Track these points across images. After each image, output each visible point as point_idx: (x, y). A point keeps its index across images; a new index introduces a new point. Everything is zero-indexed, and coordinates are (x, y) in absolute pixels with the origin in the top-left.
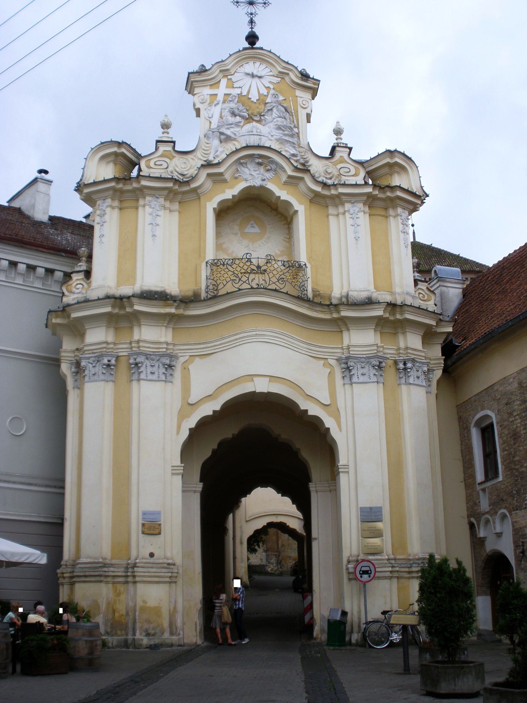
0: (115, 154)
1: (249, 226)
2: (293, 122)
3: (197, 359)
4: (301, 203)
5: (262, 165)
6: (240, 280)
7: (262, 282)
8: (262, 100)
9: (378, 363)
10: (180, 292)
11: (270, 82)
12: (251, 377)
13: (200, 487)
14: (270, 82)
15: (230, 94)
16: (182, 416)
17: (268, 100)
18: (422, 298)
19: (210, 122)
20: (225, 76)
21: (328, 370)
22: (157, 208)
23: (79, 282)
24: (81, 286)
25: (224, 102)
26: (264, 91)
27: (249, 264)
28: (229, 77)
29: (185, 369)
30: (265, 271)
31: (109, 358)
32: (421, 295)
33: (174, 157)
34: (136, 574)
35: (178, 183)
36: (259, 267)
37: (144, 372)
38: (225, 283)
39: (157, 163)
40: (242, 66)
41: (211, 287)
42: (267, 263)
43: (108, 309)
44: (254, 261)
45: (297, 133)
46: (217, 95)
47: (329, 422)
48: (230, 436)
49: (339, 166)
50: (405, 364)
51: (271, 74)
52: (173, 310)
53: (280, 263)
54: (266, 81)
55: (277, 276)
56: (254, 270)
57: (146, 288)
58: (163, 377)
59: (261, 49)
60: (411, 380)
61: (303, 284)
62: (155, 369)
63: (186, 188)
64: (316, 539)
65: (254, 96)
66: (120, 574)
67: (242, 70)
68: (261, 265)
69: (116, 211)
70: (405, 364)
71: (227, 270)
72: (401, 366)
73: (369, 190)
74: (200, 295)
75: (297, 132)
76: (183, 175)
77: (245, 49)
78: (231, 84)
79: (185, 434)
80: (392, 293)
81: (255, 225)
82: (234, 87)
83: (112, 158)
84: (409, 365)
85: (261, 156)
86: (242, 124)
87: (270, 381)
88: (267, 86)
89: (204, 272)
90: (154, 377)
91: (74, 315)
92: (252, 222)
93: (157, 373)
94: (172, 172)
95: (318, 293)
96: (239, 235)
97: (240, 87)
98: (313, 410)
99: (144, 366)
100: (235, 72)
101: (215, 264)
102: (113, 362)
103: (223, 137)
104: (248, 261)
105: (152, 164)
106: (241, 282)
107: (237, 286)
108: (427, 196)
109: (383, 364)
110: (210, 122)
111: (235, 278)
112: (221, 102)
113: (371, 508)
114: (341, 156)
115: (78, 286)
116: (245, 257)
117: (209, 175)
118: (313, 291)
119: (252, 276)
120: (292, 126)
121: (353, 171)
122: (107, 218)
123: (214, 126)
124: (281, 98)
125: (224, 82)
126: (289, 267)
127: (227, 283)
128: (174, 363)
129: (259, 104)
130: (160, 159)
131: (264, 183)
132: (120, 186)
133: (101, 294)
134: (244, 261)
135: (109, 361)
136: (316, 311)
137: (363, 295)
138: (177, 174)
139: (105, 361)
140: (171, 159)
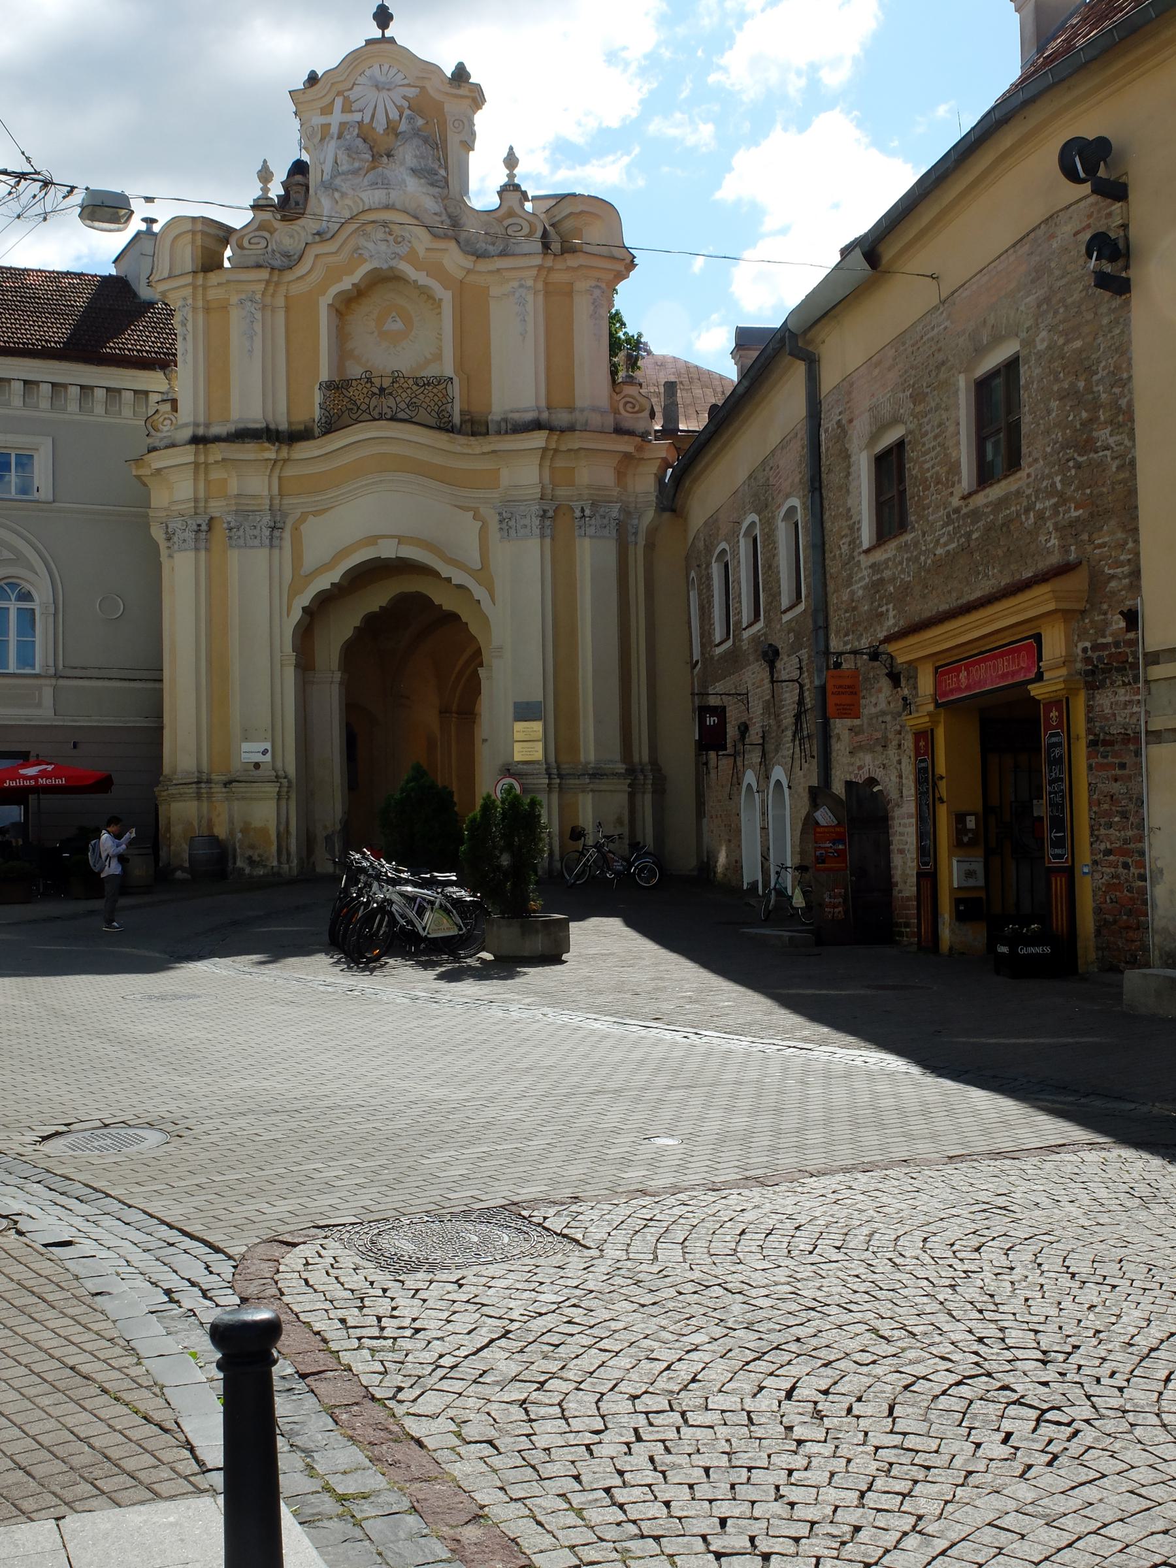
0: (194, 233)
1: (390, 320)
2: (439, 160)
3: (311, 517)
4: (446, 288)
5: (391, 235)
6: (358, 408)
7: (386, 410)
8: (392, 128)
9: (542, 513)
10: (290, 423)
11: (404, 97)
12: (372, 540)
13: (338, 676)
14: (404, 97)
15: (348, 123)
16: (294, 592)
17: (403, 127)
18: (630, 410)
19: (322, 171)
20: (339, 94)
21: (480, 523)
22: (253, 310)
23: (167, 416)
24: (169, 422)
25: (339, 137)
26: (394, 114)
27: (369, 385)
28: (346, 94)
29: (296, 529)
30: (390, 394)
31: (199, 522)
32: (629, 405)
33: (276, 230)
34: (213, 790)
35: (276, 272)
36: (382, 390)
37: (242, 539)
38: (340, 412)
39: (252, 241)
40: (363, 73)
41: (323, 421)
42: (393, 382)
43: (191, 459)
44: (377, 381)
45: (444, 177)
46: (330, 124)
47: (479, 592)
48: (375, 608)
49: (506, 223)
50: (583, 510)
51: (406, 82)
52: (273, 456)
53: (411, 382)
54: (397, 95)
55: (407, 400)
56: (375, 394)
57: (241, 426)
58: (267, 541)
59: (392, 40)
60: (591, 531)
61: (443, 408)
62: (256, 532)
63: (289, 276)
64: (485, 740)
65: (380, 125)
66: (219, 790)
67: (361, 80)
68: (385, 386)
69: (201, 317)
70: (583, 510)
71: (342, 395)
72: (578, 514)
73: (538, 260)
74: (312, 430)
75: (445, 175)
76: (289, 256)
77: (369, 42)
78: (347, 108)
79: (297, 614)
80: (571, 409)
81: (398, 319)
82: (352, 111)
83: (189, 237)
84: (587, 512)
85: (385, 224)
86: (362, 172)
87: (399, 543)
88: (398, 104)
89: (318, 397)
90: (257, 542)
91: (156, 465)
92: (394, 314)
93: (259, 538)
94: (273, 251)
95: (467, 417)
96: (376, 334)
97: (360, 111)
98: (458, 577)
99: (242, 530)
100: (354, 84)
101: (330, 386)
102: (204, 527)
103: (337, 195)
104: (367, 382)
105: (246, 243)
106: (360, 412)
107: (354, 417)
108: (634, 257)
109: (551, 514)
110: (322, 171)
111: (351, 406)
112: (336, 136)
113: (528, 703)
114: (510, 208)
115: (168, 422)
116: (363, 376)
117: (317, 256)
118: (462, 413)
119: (374, 402)
120: (436, 166)
121: (526, 231)
122: (190, 326)
123: (326, 177)
124: (420, 122)
125: (339, 102)
126: (424, 384)
127: (343, 413)
128: (278, 525)
129: (388, 134)
130: (257, 233)
131: (393, 263)
132: (200, 281)
133: (187, 433)
134: (362, 382)
135: (199, 525)
136: (459, 445)
137: (530, 416)
138: (279, 255)
139: (195, 528)
140: (271, 234)
